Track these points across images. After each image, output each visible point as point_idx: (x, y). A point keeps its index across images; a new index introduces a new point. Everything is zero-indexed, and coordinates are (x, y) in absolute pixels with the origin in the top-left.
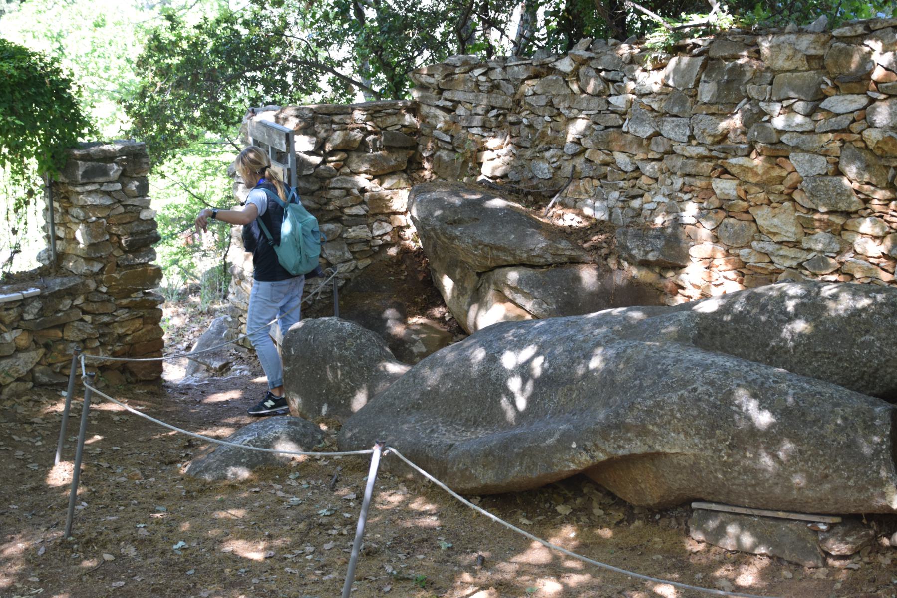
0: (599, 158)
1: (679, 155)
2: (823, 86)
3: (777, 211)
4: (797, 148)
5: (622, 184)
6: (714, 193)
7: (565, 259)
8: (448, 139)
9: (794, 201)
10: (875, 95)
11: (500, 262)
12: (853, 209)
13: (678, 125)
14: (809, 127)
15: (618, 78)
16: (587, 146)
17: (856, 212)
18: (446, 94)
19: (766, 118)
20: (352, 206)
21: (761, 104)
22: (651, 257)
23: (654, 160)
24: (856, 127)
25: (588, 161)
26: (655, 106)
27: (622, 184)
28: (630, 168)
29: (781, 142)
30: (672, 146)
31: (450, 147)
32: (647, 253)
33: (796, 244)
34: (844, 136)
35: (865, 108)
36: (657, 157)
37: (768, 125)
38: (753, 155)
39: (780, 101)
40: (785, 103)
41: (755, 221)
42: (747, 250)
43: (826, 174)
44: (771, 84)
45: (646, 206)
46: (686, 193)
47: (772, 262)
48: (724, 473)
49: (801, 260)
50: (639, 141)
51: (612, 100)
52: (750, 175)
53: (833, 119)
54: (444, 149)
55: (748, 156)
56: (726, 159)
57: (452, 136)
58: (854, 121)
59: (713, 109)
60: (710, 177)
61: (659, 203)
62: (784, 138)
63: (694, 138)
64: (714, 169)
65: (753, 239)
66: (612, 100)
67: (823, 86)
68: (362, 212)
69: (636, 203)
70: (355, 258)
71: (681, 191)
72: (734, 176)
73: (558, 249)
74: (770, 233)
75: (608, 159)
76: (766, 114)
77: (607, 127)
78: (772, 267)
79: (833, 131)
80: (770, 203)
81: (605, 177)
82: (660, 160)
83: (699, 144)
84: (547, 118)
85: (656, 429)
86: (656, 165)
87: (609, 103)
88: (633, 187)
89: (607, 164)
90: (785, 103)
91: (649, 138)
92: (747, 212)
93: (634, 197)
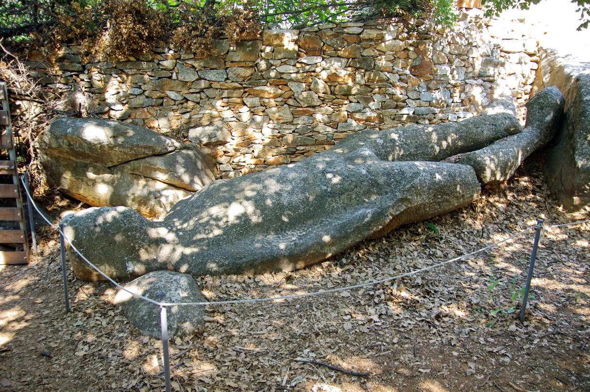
5: (175, 107)
10: (325, 56)
13: (217, 74)
17: (319, 106)
25: (147, 97)
29: (281, 78)
33: (291, 123)
38: (268, 84)
39: (280, 60)
40: (283, 60)
49: (293, 130)
52: (266, 94)
59: (243, 64)
62: (283, 76)
75: (163, 95)
81: (162, 104)
85: (410, 197)
90: (283, 60)
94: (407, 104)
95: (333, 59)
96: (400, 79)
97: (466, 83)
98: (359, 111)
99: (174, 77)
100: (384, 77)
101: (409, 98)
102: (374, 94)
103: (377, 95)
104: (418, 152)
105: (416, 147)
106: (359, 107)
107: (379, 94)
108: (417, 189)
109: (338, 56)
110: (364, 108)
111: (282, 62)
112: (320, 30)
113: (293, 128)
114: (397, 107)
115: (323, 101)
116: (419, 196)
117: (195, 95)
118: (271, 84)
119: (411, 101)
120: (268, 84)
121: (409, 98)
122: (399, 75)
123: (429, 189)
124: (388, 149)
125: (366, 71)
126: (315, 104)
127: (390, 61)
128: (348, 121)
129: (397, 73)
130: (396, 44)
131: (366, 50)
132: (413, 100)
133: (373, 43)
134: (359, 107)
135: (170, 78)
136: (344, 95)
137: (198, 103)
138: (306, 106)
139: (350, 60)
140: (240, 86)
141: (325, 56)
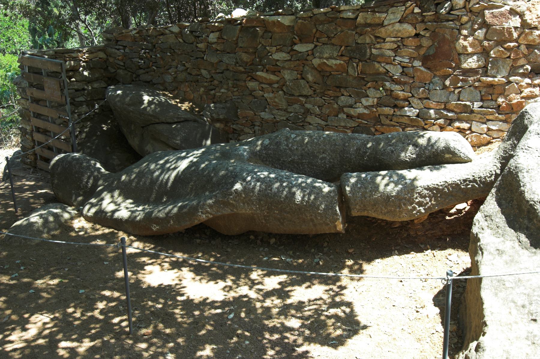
0: (194, 72)
1: (231, 71)
2: (294, 40)
3: (276, 95)
4: (284, 68)
5: (205, 84)
6: (248, 88)
7: (182, 120)
8: (122, 64)
9: (283, 90)
11: (153, 122)
12: (309, 94)
14: (289, 58)
15: (200, 35)
16: (188, 67)
17: (310, 95)
18: (119, 43)
19: (269, 54)
20: (78, 97)
21: (267, 48)
22: (221, 117)
23: (219, 73)
24: (309, 58)
26: (218, 48)
27: (205, 84)
28: (208, 77)
29: (277, 65)
30: (227, 66)
31: (124, 68)
32: (219, 115)
34: (304, 62)
35: (313, 49)
36: (221, 71)
37: (270, 57)
39: (276, 46)
40: (278, 47)
41: (266, 100)
42: (263, 113)
43: (297, 79)
44: (271, 38)
45: (217, 94)
46: (235, 88)
47: (275, 118)
48: (265, 220)
50: (212, 64)
51: (199, 45)
53: (300, 54)
54: (121, 69)
55: (263, 71)
56: (253, 72)
57: (124, 63)
58: (308, 55)
60: (245, 81)
61: (223, 93)
62: (278, 63)
63: (237, 63)
64: (248, 77)
65: (266, 108)
66: (199, 45)
67: (294, 40)
68: (84, 100)
69: (213, 92)
70: (82, 121)
71: (233, 87)
72: (256, 80)
73: (179, 115)
74: (274, 105)
75: (198, 73)
76: (269, 52)
77: (197, 58)
78: (275, 120)
79: (299, 60)
80: (273, 92)
82: (222, 73)
83: (240, 66)
84: (169, 54)
86: (221, 75)
87: (197, 47)
88: (211, 85)
89: (199, 75)
90: (278, 47)
91: (217, 63)
92: (263, 96)
93: (212, 90)
94: (410, 104)
95: (326, 46)
96: (403, 72)
97: (509, 82)
98: (351, 106)
99: (205, 57)
100: (381, 69)
101: (413, 96)
102: (369, 88)
103: (371, 89)
104: (304, 161)
105: (302, 155)
106: (351, 101)
107: (374, 88)
108: (241, 196)
109: (333, 45)
111: (277, 49)
112: (314, 15)
113: (288, 115)
114: (395, 106)
115: (314, 91)
116: (246, 204)
117: (219, 75)
118: (267, 71)
119: (415, 100)
120: (265, 70)
121: (413, 96)
122: (403, 67)
123: (260, 200)
124: (270, 152)
125: (360, 60)
126: (304, 93)
127: (392, 50)
128: (339, 116)
129: (399, 64)
130: (401, 28)
131: (361, 37)
132: (420, 99)
133: (369, 29)
134: (351, 101)
135: (203, 58)
136: (337, 87)
137: (221, 82)
138: (298, 94)
139: (343, 48)
140: (243, 70)
141: (318, 44)
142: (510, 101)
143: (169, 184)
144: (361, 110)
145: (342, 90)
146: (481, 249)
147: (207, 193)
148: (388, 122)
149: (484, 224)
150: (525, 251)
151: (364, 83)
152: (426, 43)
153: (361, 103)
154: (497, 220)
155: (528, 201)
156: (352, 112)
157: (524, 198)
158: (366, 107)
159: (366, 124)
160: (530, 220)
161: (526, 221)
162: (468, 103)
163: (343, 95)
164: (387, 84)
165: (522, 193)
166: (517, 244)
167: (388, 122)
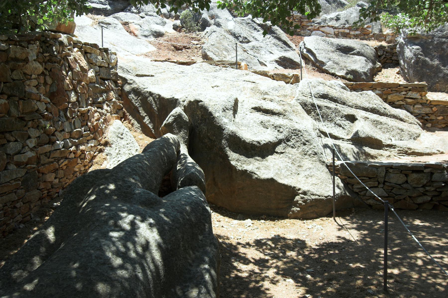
98: (19, 153)
102: (29, 128)
106: (19, 146)
107: (32, 127)
110: (23, 147)
134: (19, 146)
142: (93, 124)
143: (162, 272)
144: (30, 154)
145: (8, 135)
146: (253, 173)
147: (200, 237)
148: (47, 160)
149: (239, 164)
150: (263, 162)
151: (25, 123)
152: (49, 81)
153: (28, 146)
154: (242, 159)
155: (249, 143)
156: (23, 158)
157: (246, 142)
158: (32, 150)
159: (34, 168)
160: (254, 150)
161: (253, 152)
162: (79, 129)
163: (9, 141)
164: (41, 120)
165: (244, 141)
166: (258, 162)
167: (47, 160)
